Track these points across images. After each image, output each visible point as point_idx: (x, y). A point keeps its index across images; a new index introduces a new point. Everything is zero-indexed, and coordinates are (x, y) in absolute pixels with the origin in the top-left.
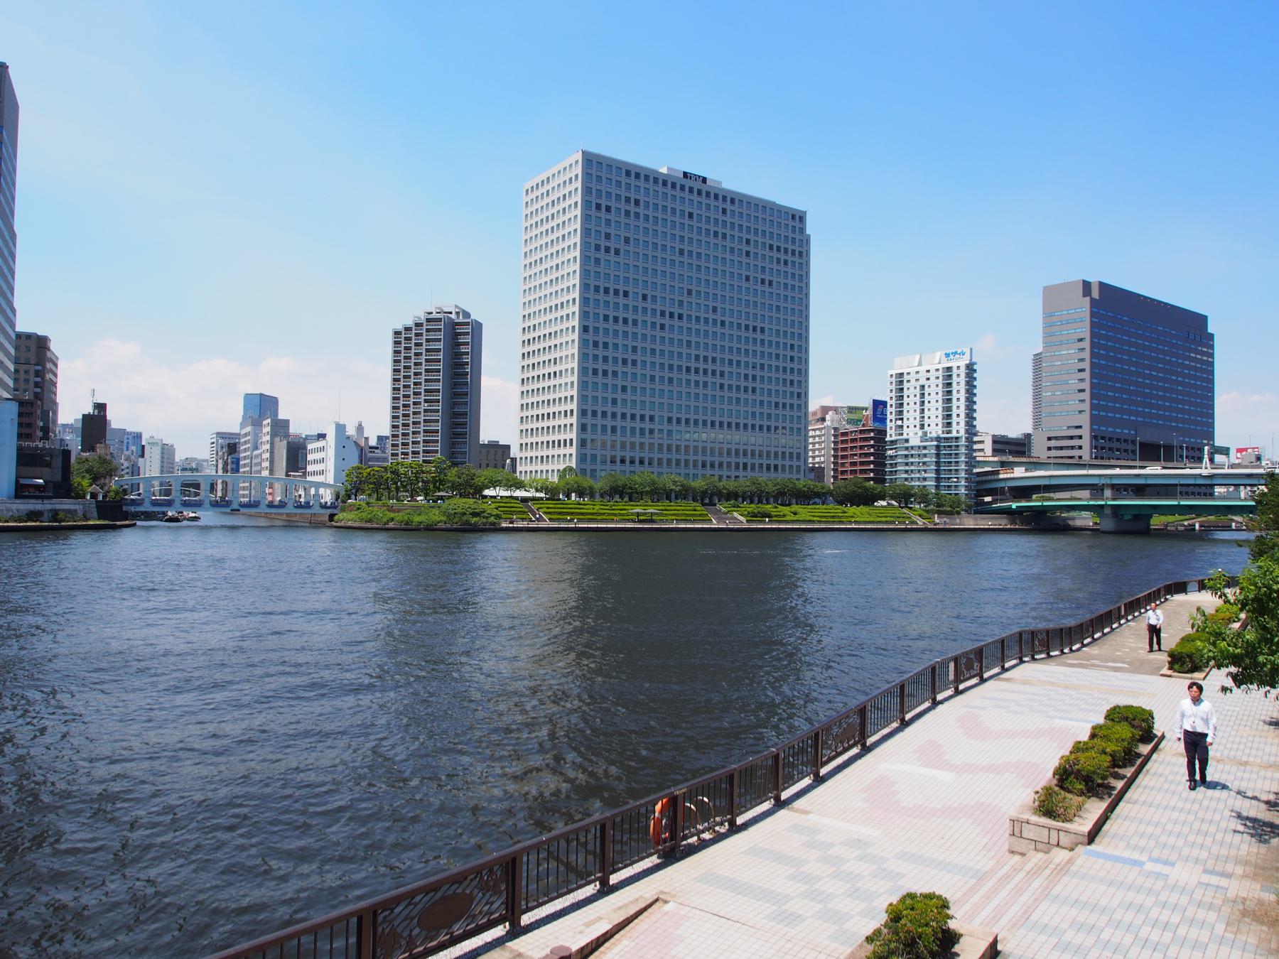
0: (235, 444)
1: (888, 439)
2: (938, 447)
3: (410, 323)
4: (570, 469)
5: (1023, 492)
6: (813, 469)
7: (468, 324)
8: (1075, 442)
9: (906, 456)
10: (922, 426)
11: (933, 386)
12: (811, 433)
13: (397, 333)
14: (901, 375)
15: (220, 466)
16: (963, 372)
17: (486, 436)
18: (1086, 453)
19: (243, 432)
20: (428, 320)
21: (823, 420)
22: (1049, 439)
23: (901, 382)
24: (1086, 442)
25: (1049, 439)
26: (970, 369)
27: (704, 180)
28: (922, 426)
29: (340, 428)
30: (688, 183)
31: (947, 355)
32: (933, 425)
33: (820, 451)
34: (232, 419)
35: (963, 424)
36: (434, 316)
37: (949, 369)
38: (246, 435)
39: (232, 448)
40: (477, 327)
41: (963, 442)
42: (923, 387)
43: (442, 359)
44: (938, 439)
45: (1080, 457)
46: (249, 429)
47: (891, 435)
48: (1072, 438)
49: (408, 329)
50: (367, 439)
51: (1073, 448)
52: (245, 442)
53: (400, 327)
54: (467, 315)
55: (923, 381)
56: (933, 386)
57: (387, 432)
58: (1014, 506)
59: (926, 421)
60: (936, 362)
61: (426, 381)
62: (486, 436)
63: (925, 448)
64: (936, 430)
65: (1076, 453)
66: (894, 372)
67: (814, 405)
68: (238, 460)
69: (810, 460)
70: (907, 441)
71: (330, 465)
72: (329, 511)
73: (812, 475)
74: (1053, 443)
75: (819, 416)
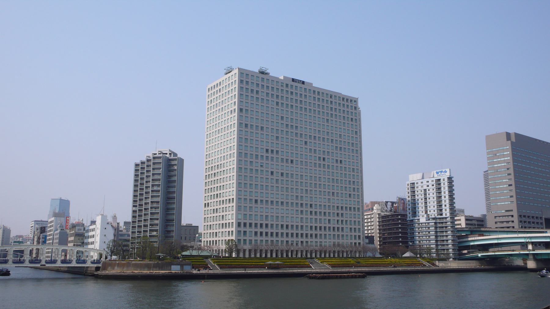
0: (45, 228)
1: (408, 219)
2: (436, 223)
3: (144, 159)
4: (232, 240)
5: (485, 247)
6: (367, 237)
7: (175, 159)
8: (510, 219)
10: (426, 212)
11: (431, 190)
12: (366, 217)
13: (137, 165)
14: (413, 184)
15: (36, 239)
16: (446, 180)
17: (184, 222)
18: (516, 224)
19: (49, 221)
20: (154, 158)
21: (373, 209)
23: (414, 188)
24: (516, 219)
26: (450, 179)
27: (303, 83)
28: (426, 212)
29: (104, 217)
30: (294, 84)
31: (437, 173)
32: (432, 211)
33: (372, 227)
34: (45, 214)
35: (448, 210)
38: (51, 222)
39: (43, 230)
40: (181, 161)
43: (161, 179)
45: (513, 227)
46: (53, 219)
47: (410, 217)
49: (143, 163)
50: (118, 224)
52: (51, 226)
53: (138, 162)
54: (175, 155)
55: (425, 187)
57: (129, 219)
58: (480, 255)
62: (184, 222)
63: (428, 223)
64: (433, 212)
65: (510, 224)
66: (409, 183)
67: (367, 200)
68: (46, 236)
69: (366, 232)
71: (97, 239)
72: (96, 265)
73: (367, 241)
74: (498, 219)
75: (370, 207)
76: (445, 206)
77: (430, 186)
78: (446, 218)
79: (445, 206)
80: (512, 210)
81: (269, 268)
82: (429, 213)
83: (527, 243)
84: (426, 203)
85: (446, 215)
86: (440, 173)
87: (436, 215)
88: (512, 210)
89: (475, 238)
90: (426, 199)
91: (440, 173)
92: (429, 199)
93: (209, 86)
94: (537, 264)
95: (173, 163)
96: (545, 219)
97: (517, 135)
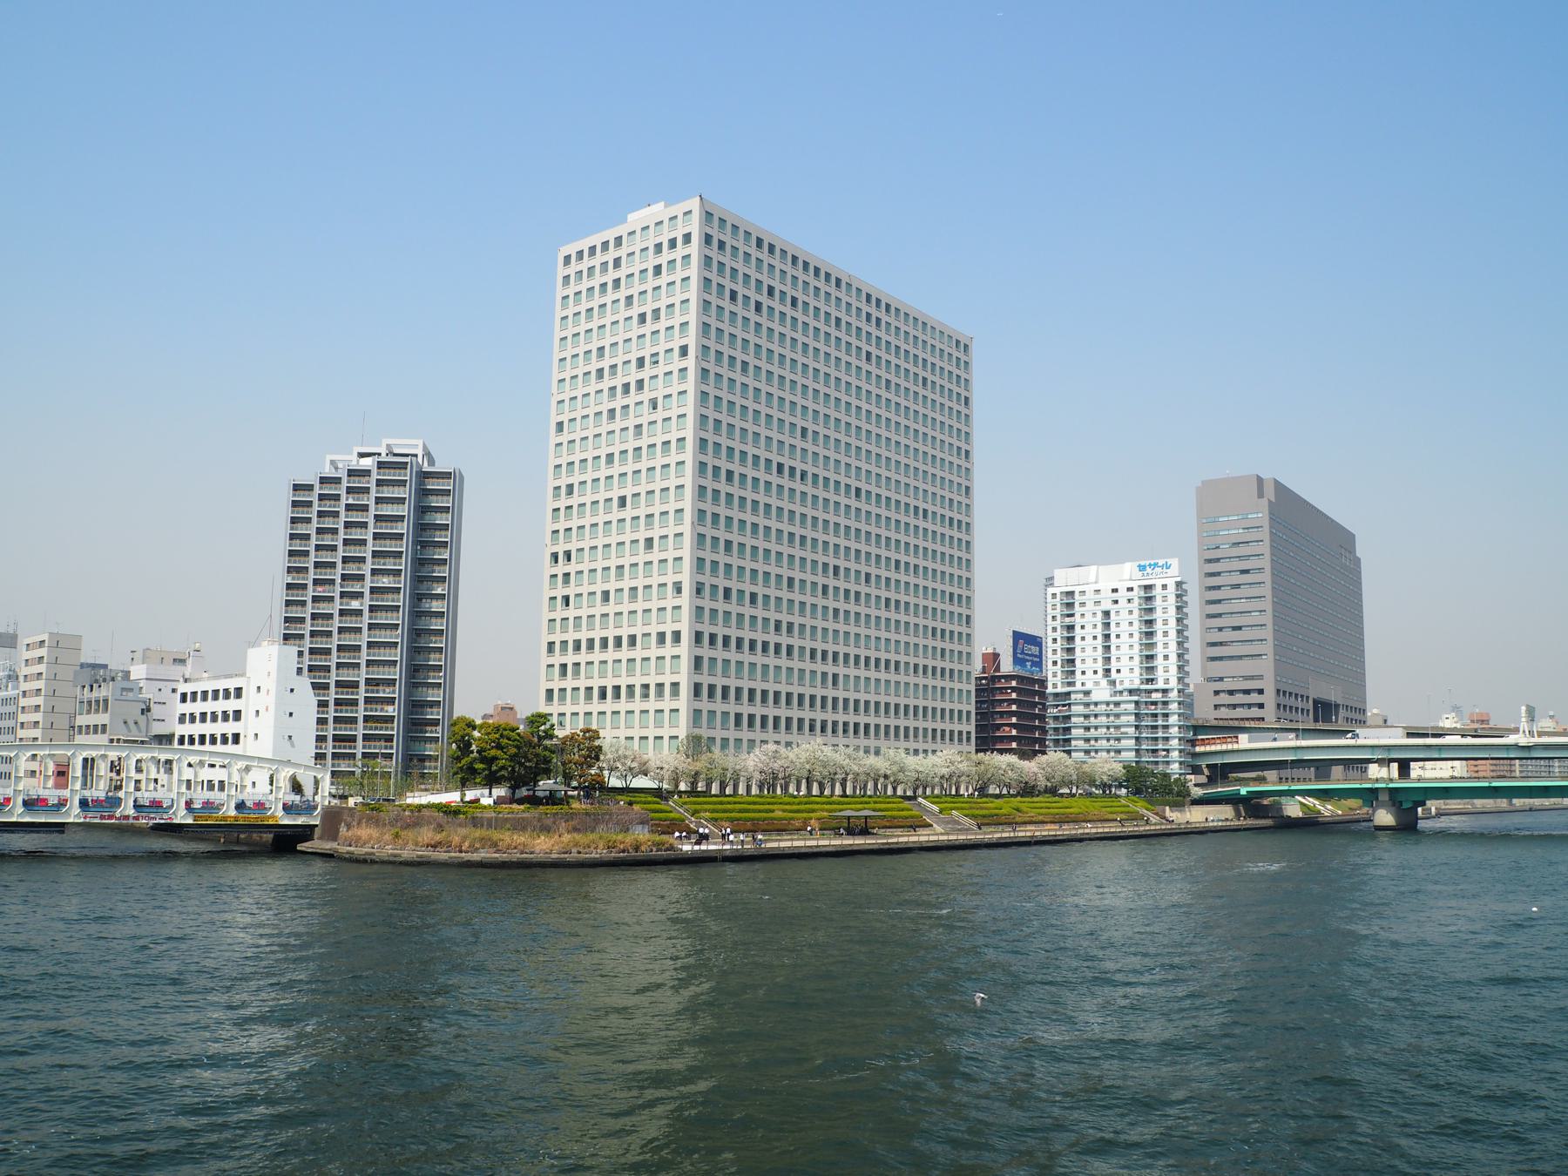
1: (1050, 690)
2: (1137, 703)
9: (1086, 717)
14: (1071, 594)
16: (1172, 588)
18: (1270, 713)
22: (1217, 693)
23: (1070, 605)
24: (1269, 699)
25: (1217, 693)
31: (1142, 568)
36: (383, 458)
37: (1148, 588)
41: (1173, 695)
42: (1107, 614)
44: (1131, 692)
47: (1055, 682)
48: (1247, 692)
51: (1250, 706)
55: (1107, 605)
56: (1124, 615)
58: (1243, 791)
59: (1114, 665)
60: (1126, 574)
61: (374, 572)
63: (1117, 704)
64: (1130, 676)
66: (1057, 591)
70: (1087, 693)
74: (1225, 699)
76: (1166, 657)
77: (1123, 602)
78: (1165, 691)
79: (1166, 657)
80: (1260, 677)
81: (851, 832)
82: (1114, 674)
83: (1369, 761)
84: (1107, 648)
85: (1167, 681)
86: (1149, 570)
87: (1137, 682)
88: (1260, 677)
89: (1224, 747)
90: (1107, 637)
91: (1149, 570)
92: (1118, 636)
93: (571, 249)
94: (1397, 817)
95: (432, 485)
96: (1316, 702)
97: (1278, 485)
